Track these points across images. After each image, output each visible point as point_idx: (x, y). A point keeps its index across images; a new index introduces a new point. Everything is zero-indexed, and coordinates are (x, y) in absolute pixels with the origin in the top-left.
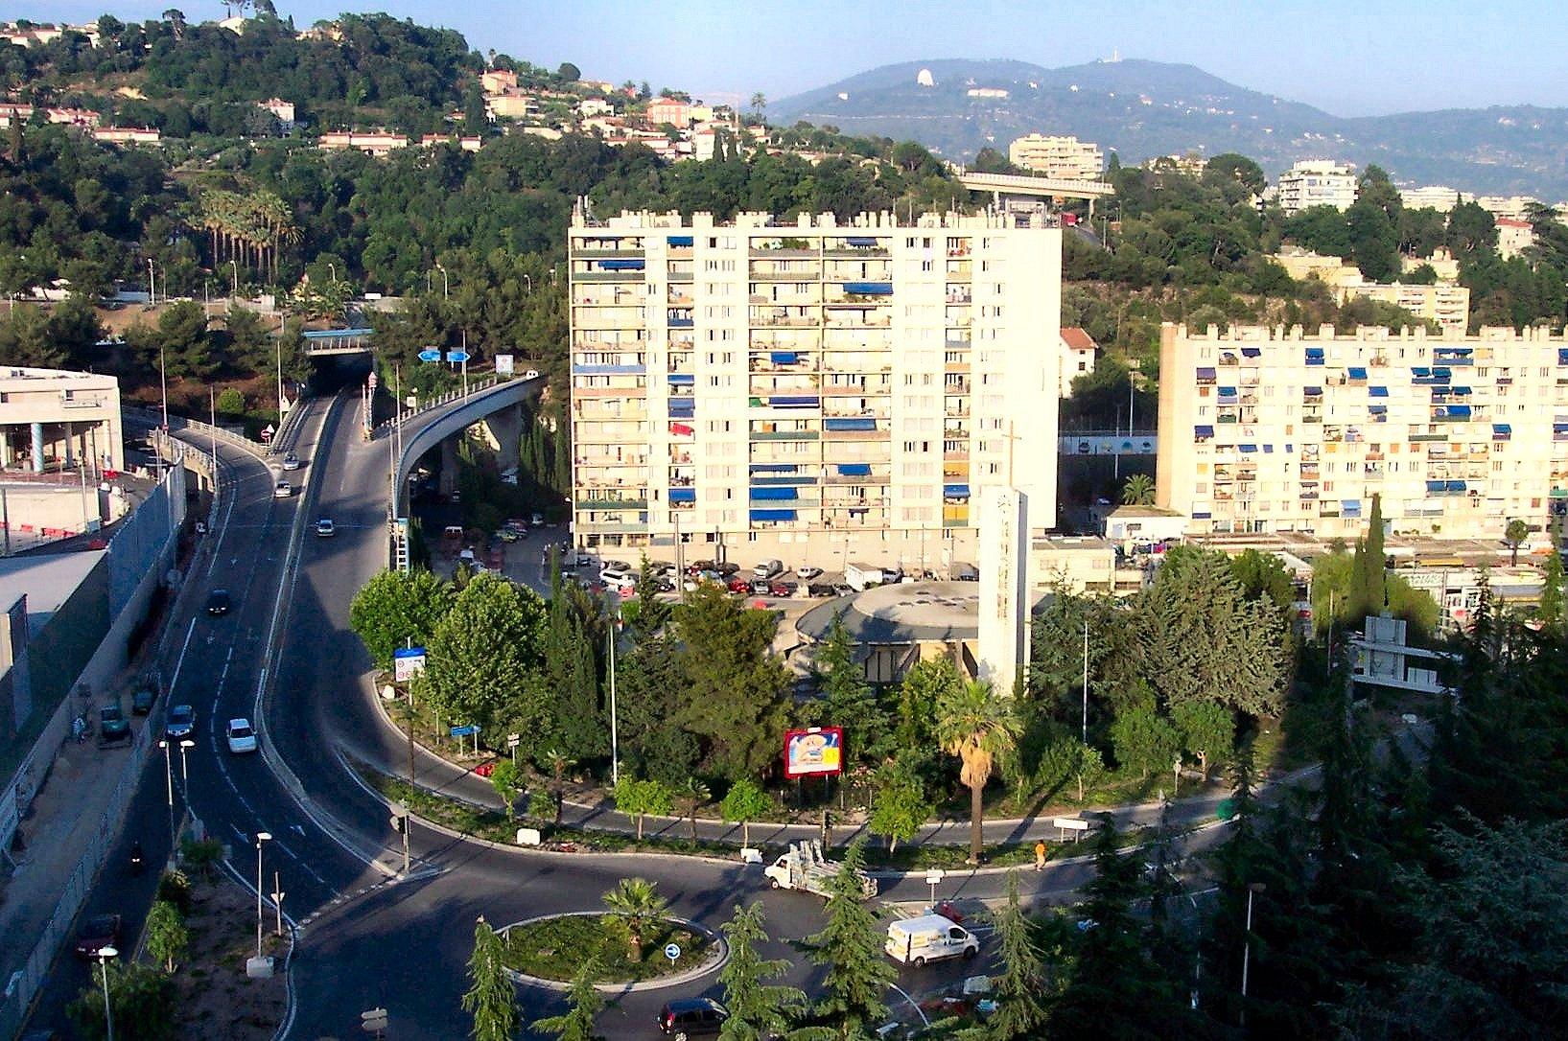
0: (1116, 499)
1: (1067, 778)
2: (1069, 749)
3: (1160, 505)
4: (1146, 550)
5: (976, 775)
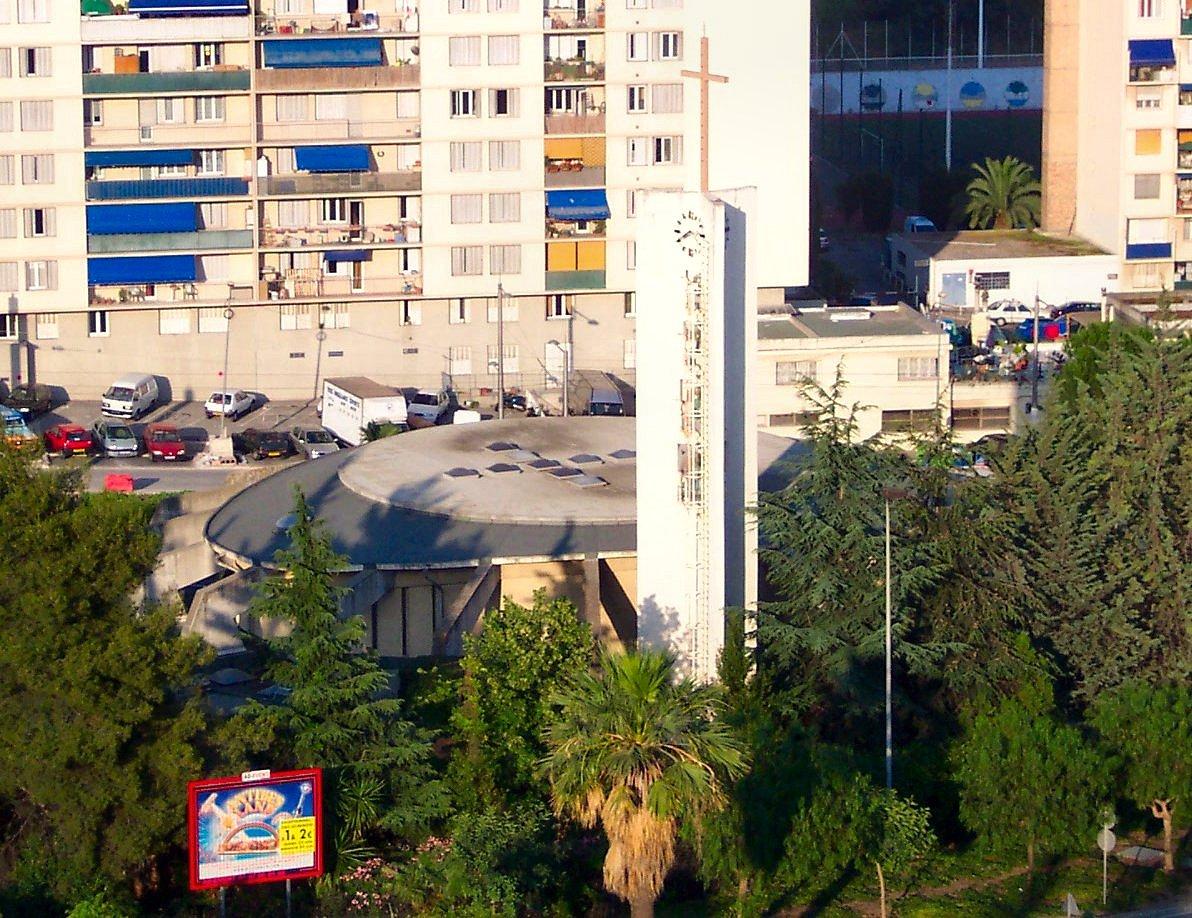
0: (950, 218)
1: (849, 874)
2: (853, 804)
3: (1053, 227)
4: (1022, 334)
5: (639, 869)
